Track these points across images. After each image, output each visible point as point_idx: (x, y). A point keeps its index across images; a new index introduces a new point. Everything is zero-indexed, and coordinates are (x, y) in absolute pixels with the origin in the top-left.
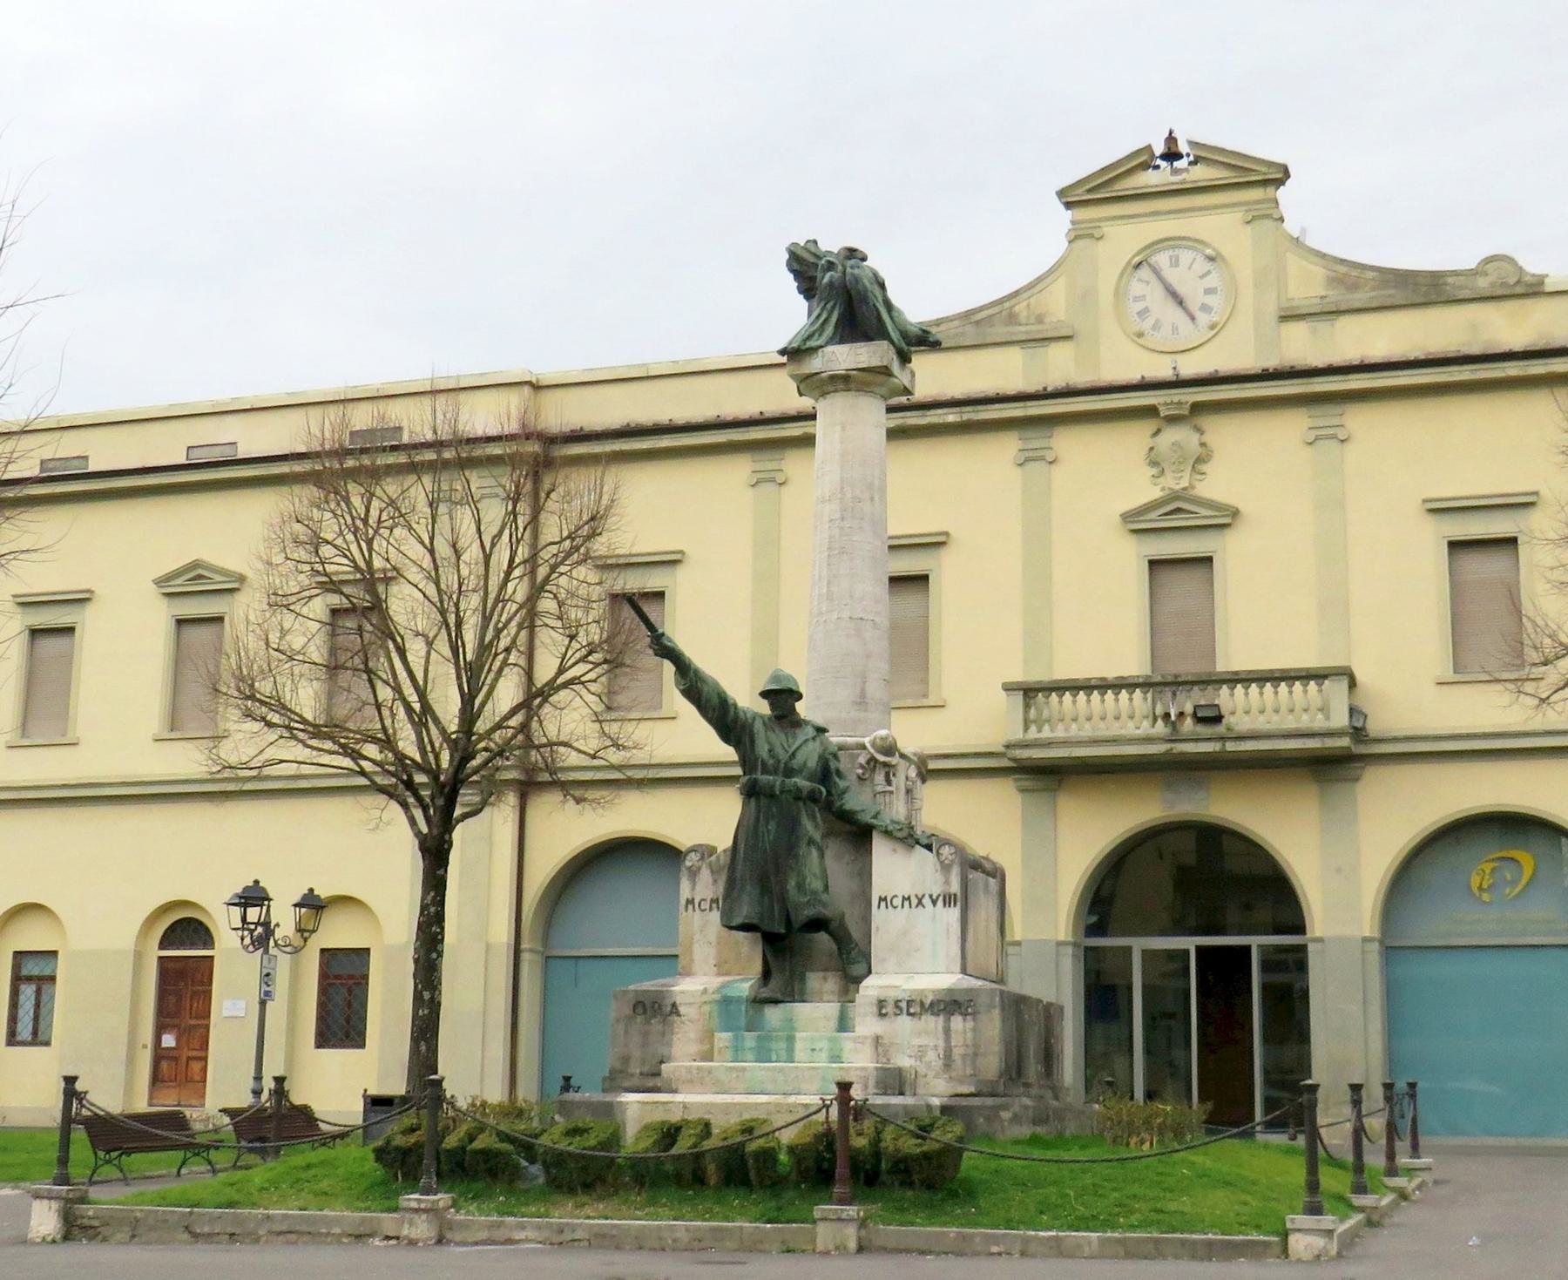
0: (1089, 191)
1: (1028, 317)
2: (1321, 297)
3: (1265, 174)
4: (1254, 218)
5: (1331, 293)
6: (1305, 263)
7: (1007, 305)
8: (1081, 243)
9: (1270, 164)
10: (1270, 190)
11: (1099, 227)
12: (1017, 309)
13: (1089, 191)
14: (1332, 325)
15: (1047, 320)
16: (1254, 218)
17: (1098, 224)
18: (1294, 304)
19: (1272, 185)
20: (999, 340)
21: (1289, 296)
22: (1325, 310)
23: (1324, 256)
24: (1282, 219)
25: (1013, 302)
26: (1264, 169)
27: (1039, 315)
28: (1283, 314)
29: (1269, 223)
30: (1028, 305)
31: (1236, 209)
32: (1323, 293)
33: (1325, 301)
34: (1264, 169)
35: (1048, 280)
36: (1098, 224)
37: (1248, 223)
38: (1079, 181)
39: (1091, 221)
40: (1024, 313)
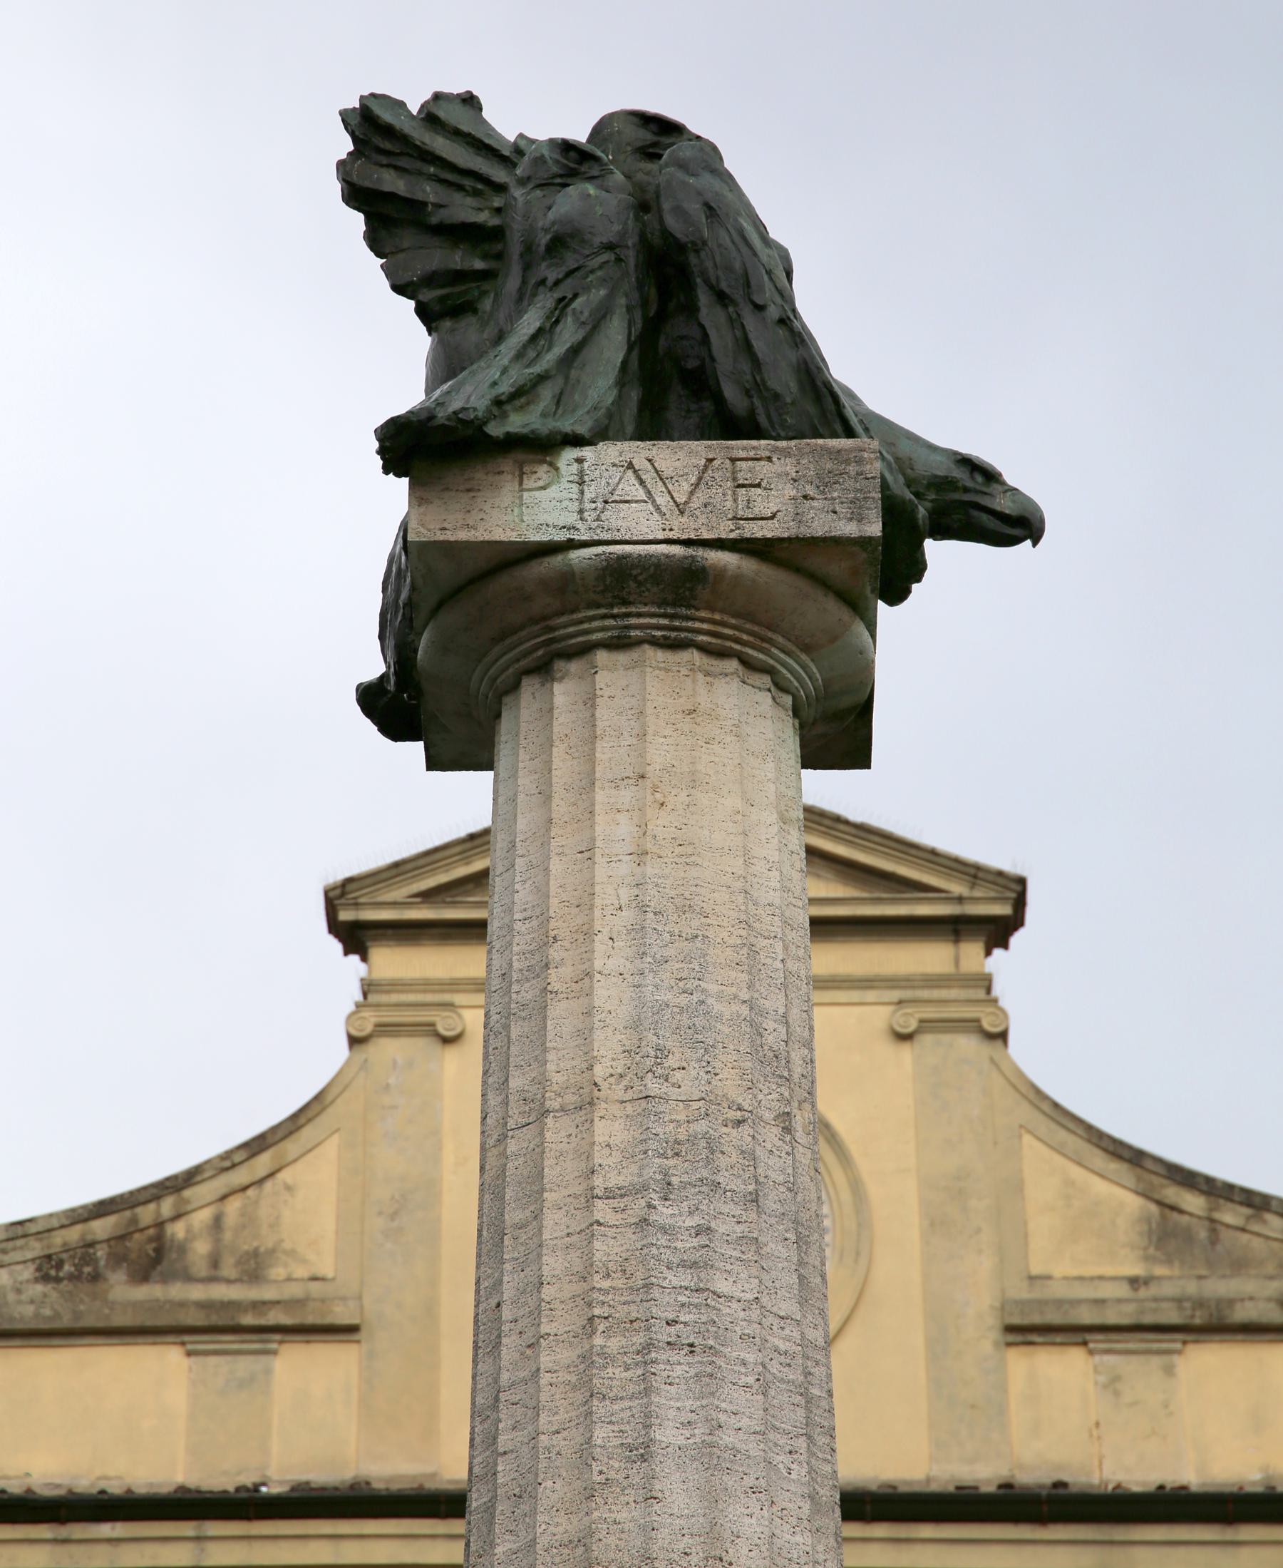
0: (428, 896)
1: (215, 1261)
2: (1134, 1282)
3: (960, 900)
4: (927, 1026)
5: (1160, 1271)
6: (1076, 1172)
7: (146, 1214)
8: (388, 1049)
9: (974, 873)
10: (971, 951)
11: (449, 1006)
12: (178, 1230)
13: (428, 896)
14: (1169, 1371)
15: (278, 1272)
16: (927, 1026)
17: (446, 997)
18: (1058, 1290)
19: (972, 936)
20: (119, 1320)
21: (1036, 1270)
22: (1148, 1319)
23: (1134, 1157)
24: (1003, 1036)
25: (167, 1206)
26: (957, 888)
27: (255, 1253)
28: (1016, 1320)
29: (967, 1044)
30: (217, 1222)
31: (871, 995)
32: (1137, 1270)
33: (1143, 1293)
34: (957, 888)
35: (291, 1147)
36: (446, 997)
37: (904, 1037)
38: (396, 865)
39: (427, 985)
40: (201, 1248)
